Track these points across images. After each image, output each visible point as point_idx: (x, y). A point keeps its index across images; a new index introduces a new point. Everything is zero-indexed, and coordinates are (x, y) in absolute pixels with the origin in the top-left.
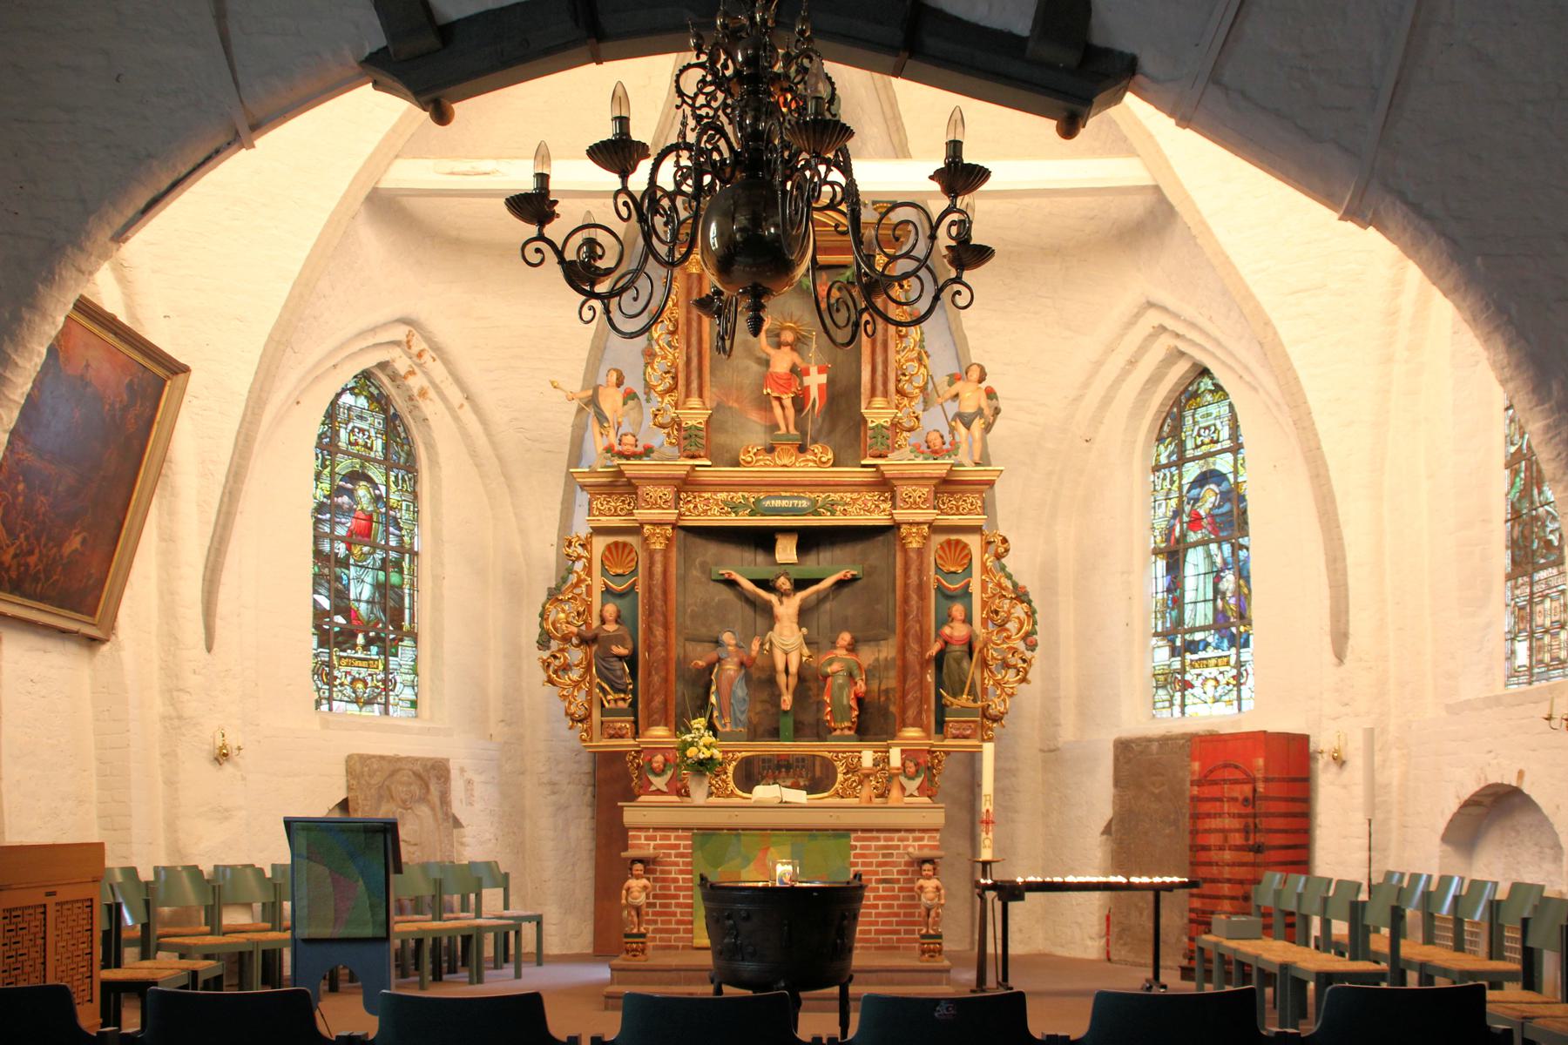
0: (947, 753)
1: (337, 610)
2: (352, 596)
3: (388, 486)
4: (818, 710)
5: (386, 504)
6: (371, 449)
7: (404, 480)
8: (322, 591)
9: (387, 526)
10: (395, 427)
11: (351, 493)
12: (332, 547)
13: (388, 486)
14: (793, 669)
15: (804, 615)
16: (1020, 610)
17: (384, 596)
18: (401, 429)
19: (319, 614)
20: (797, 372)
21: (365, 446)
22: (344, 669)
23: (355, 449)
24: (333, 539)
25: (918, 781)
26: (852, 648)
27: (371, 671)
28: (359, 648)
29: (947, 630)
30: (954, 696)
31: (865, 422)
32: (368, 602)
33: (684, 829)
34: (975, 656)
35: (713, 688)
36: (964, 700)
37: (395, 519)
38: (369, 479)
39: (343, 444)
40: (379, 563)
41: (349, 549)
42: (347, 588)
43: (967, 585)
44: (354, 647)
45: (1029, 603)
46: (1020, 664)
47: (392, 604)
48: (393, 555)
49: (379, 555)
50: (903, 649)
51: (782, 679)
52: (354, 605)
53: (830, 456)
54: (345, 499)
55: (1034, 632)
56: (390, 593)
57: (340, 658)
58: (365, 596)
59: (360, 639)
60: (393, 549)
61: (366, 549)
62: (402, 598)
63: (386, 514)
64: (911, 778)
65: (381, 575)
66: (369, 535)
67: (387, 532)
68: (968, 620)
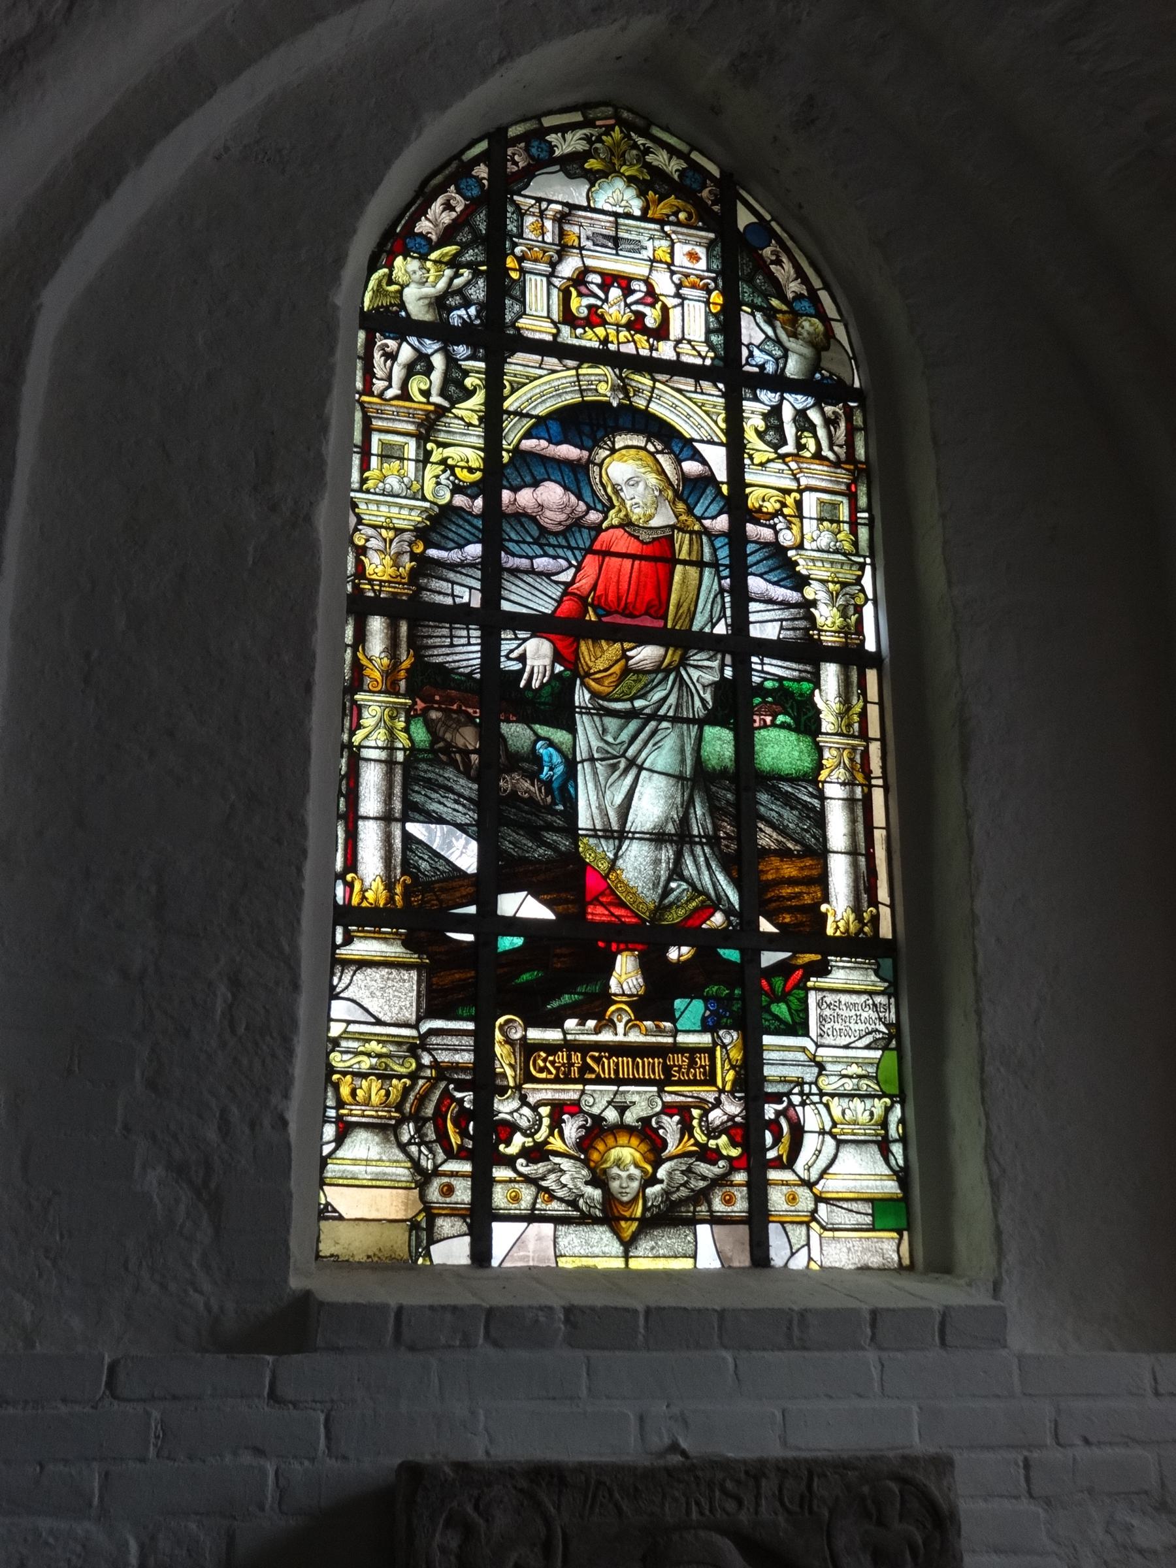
1: (499, 872)
6: (661, 332)
8: (445, 807)
9: (739, 572)
10: (762, 267)
21: (636, 324)
23: (590, 339)
32: (657, 838)
37: (776, 550)
40: (702, 701)
44: (596, 1006)
49: (705, 672)
52: (597, 853)
54: (551, 494)
57: (528, 1049)
59: (626, 975)
60: (767, 648)
61: (646, 655)
62: (820, 820)
65: (719, 744)
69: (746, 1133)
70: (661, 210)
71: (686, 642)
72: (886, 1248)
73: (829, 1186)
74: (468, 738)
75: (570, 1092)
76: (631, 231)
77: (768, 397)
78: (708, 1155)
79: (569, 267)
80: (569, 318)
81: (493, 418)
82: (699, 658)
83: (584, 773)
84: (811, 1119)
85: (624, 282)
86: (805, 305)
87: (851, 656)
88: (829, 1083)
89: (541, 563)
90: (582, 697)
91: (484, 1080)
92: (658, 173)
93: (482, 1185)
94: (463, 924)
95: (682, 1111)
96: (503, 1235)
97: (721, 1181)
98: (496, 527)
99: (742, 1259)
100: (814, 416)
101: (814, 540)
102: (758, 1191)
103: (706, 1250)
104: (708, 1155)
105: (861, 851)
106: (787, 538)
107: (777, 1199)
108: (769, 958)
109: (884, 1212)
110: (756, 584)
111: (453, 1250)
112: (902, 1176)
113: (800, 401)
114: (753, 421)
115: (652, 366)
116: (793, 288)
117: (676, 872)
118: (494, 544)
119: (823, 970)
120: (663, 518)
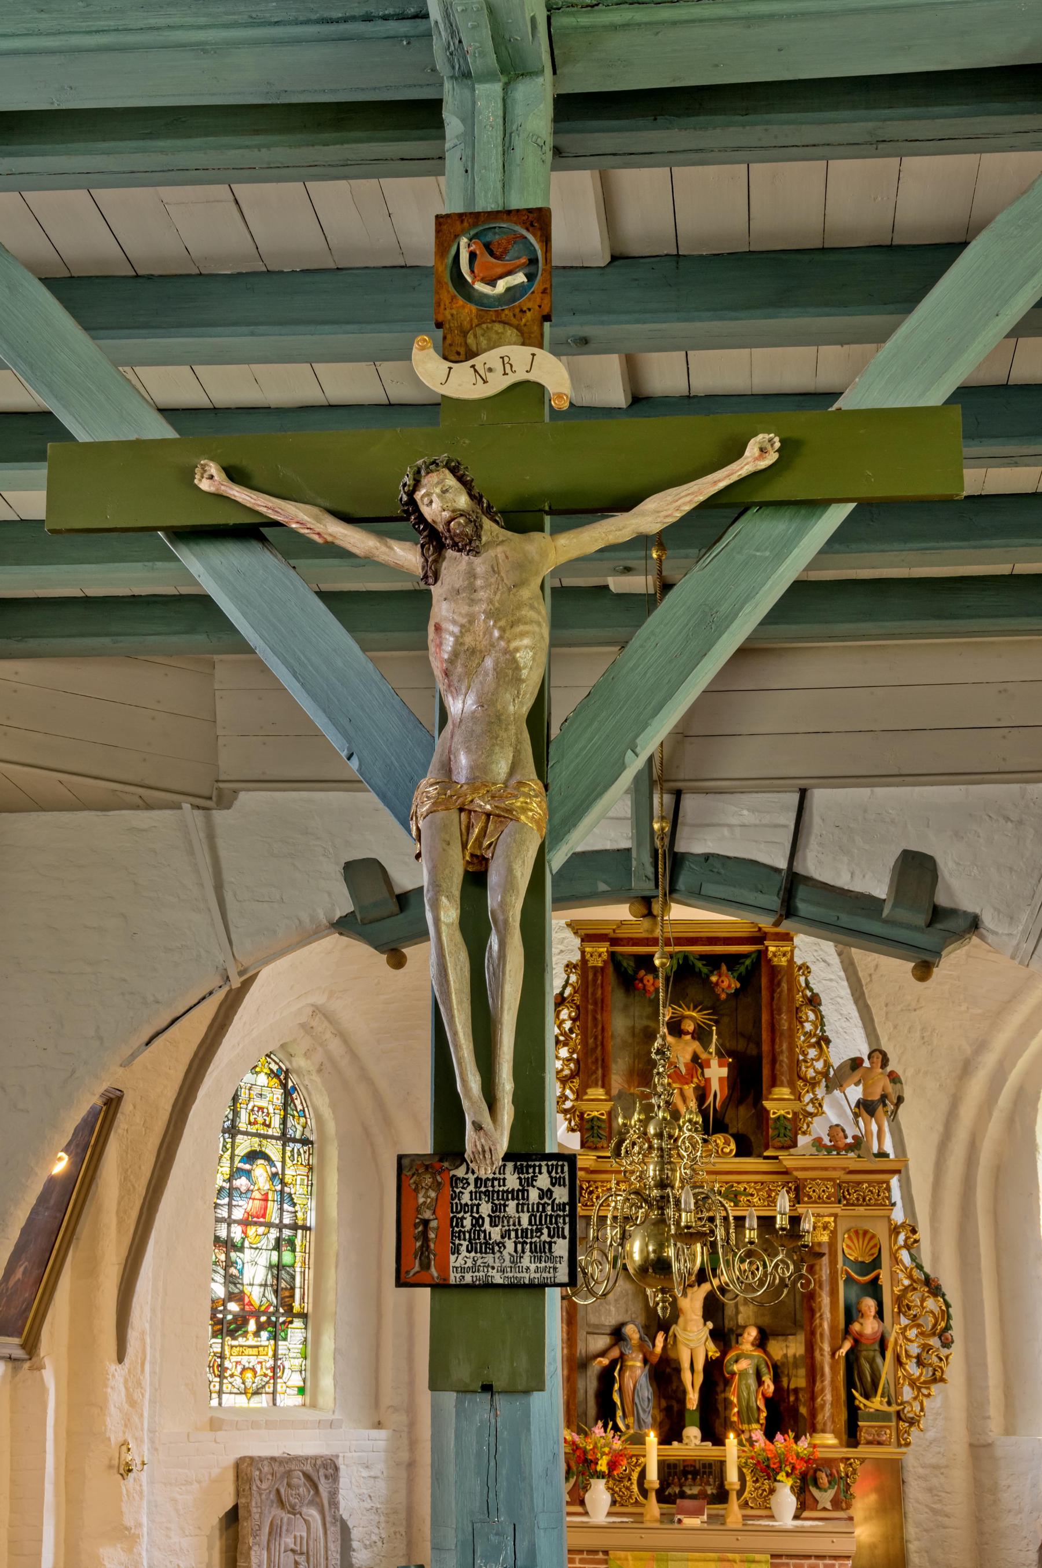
0: (862, 1460)
1: (231, 1297)
2: (246, 1281)
3: (284, 1162)
4: (726, 1408)
5: (283, 1183)
6: (269, 1126)
7: (299, 1154)
9: (282, 1203)
10: (292, 1100)
11: (248, 1173)
12: (229, 1232)
13: (284, 1162)
14: (700, 1365)
15: (712, 1308)
16: (930, 1304)
17: (277, 1277)
18: (298, 1102)
19: (216, 1306)
20: (698, 1063)
21: (264, 1124)
22: (234, 1359)
23: (252, 1129)
24: (229, 1222)
25: (831, 1494)
26: (761, 1343)
27: (261, 1358)
28: (250, 1336)
29: (856, 1327)
30: (867, 1397)
31: (768, 1112)
33: (590, 1552)
34: (889, 1354)
35: (616, 1386)
36: (877, 1403)
37: (290, 1195)
38: (266, 1157)
39: (242, 1126)
41: (244, 1232)
42: (241, 1272)
43: (877, 1278)
45: (943, 1296)
46: (935, 1359)
47: (283, 1284)
48: (287, 1233)
49: (274, 1233)
50: (810, 1347)
51: (687, 1376)
52: (247, 1290)
53: (733, 1146)
55: (948, 1327)
56: (284, 1274)
57: (232, 1347)
58: (257, 1281)
59: (252, 1326)
60: (286, 1226)
61: (261, 1230)
62: (293, 1277)
63: (282, 1192)
64: (826, 1491)
66: (264, 1216)
67: (281, 1209)
68: (880, 1314)
69: (274, 1369)
70: (272, 1083)
71: (269, 1225)
72: (299, 1400)
73: (289, 1384)
74: (223, 1257)
75: (239, 1358)
76: (266, 1091)
77: (291, 1145)
78: (265, 1375)
79: (250, 1107)
80: (250, 1123)
81: (232, 1158)
82: (272, 1230)
83: (246, 1265)
84: (287, 1364)
85: (261, 1109)
86: (301, 1113)
87: (306, 1228)
88: (291, 1355)
89: (241, 1203)
90: (247, 1244)
91: (222, 1356)
92: (271, 1070)
93: (221, 1383)
94: (221, 1312)
95: (261, 1363)
96: (224, 1397)
97: (267, 1383)
98: (231, 1192)
99: (271, 1404)
100: (301, 1151)
101: (298, 1190)
102: (275, 1384)
103: (262, 1402)
104: (265, 1375)
105: (302, 1288)
106: (293, 1192)
107: (279, 1386)
108: (282, 1319)
109: (302, 1390)
110: (286, 1207)
111: (214, 1403)
112: (304, 1381)
113: (299, 1145)
114: (288, 1154)
115: (266, 1137)
116: (300, 1107)
117: (264, 1296)
118: (230, 1196)
119: (291, 1322)
120: (267, 1187)
